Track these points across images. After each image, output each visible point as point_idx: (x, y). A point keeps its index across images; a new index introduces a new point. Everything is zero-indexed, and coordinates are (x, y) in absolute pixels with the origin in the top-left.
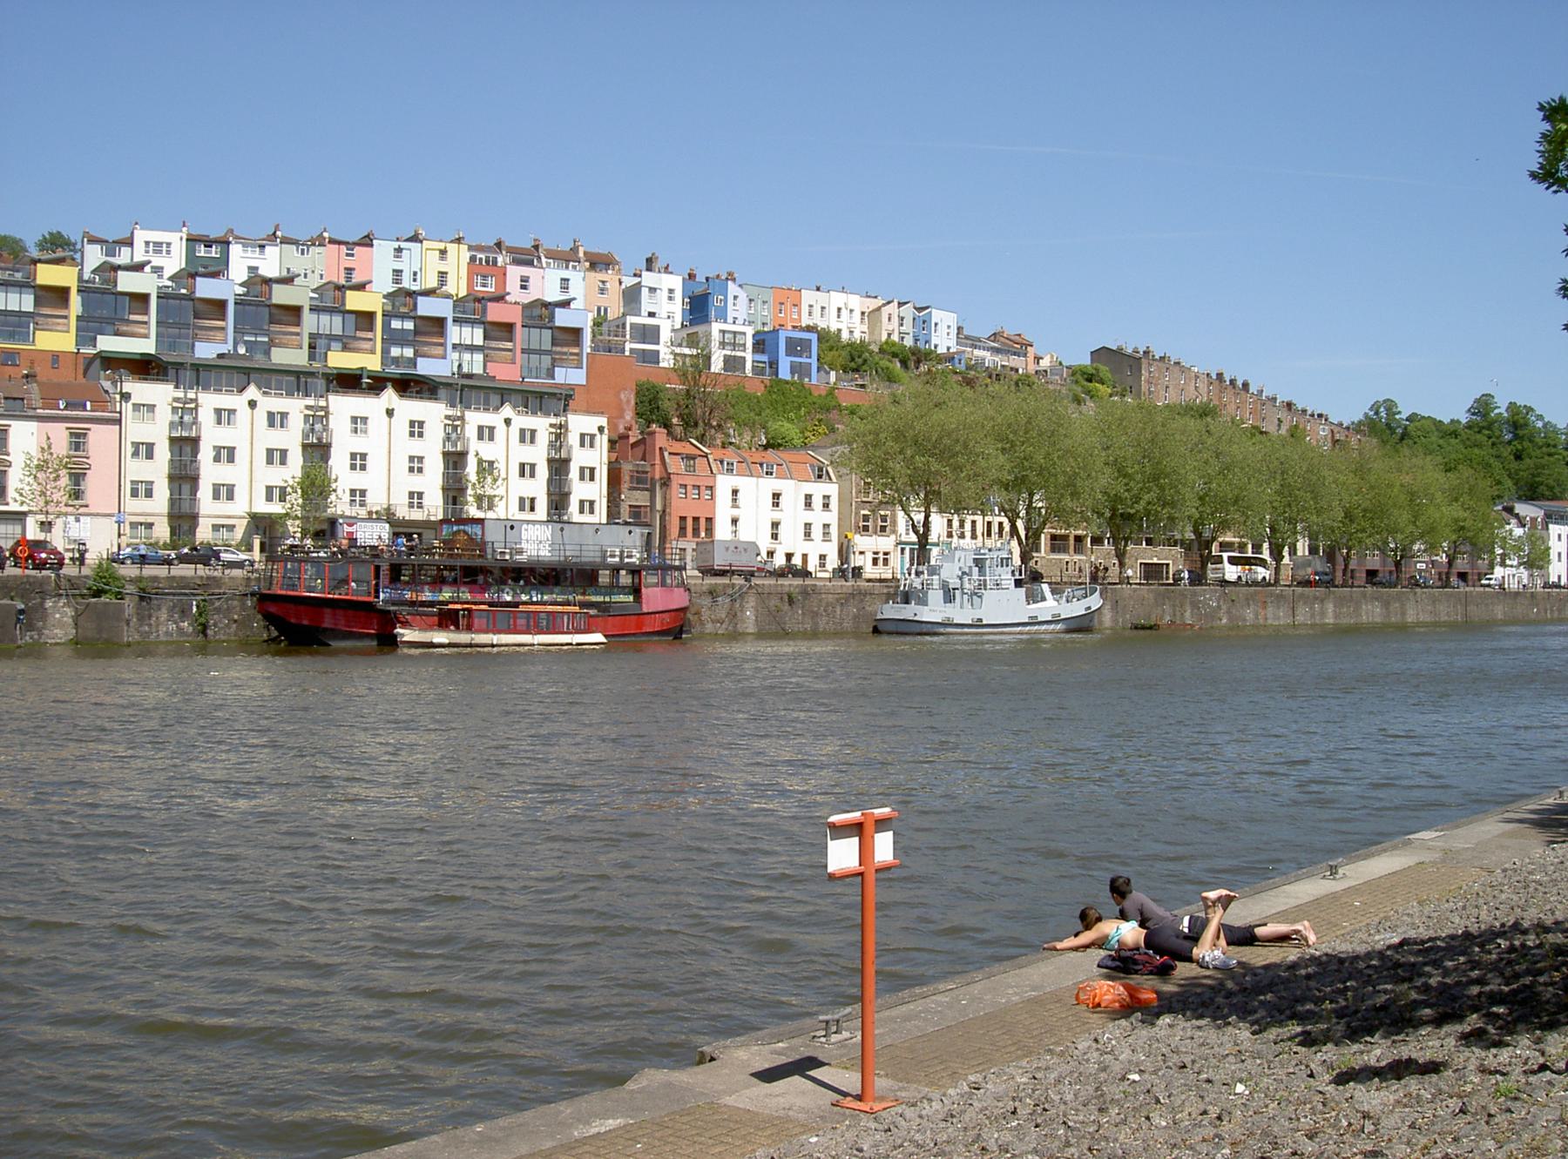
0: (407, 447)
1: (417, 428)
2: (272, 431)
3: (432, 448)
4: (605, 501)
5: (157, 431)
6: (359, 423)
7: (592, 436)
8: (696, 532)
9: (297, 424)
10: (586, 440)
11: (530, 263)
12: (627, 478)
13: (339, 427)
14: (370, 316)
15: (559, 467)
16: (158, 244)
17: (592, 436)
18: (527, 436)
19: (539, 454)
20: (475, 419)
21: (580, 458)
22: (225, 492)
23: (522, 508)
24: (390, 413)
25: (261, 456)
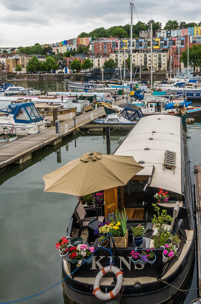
4: (167, 64)
6: (134, 56)
15: (160, 59)
16: (164, 32)
17: (165, 56)
20: (148, 55)
21: (163, 58)
23: (149, 65)
24: (137, 55)
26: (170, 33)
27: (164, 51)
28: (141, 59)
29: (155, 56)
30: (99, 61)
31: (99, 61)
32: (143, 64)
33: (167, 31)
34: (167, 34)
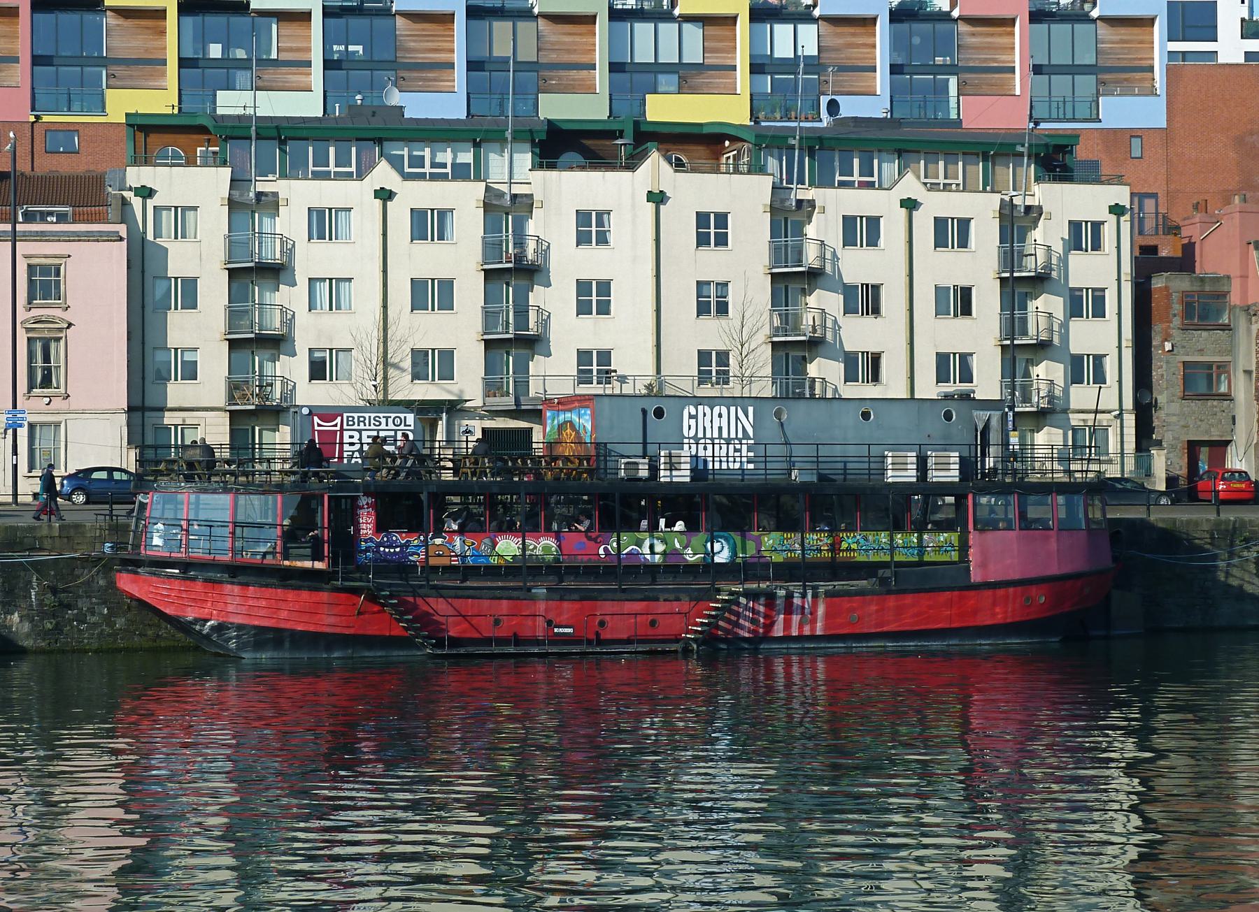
0: (690, 265)
1: (712, 229)
2: (422, 247)
5: (199, 256)
6: (591, 228)
7: (1097, 226)
9: (469, 224)
10: (1082, 236)
12: (1177, 308)
13: (551, 229)
14: (732, 20)
17: (1097, 226)
18: (952, 233)
19: (978, 265)
25: (401, 295)
28: (713, 264)
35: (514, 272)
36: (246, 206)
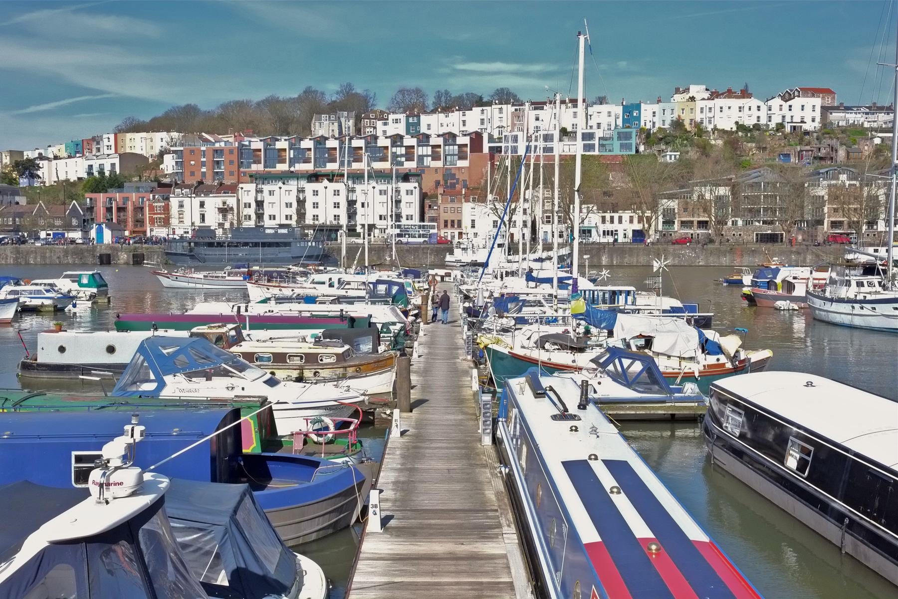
3: (342, 200)
5: (250, 198)
8: (453, 226)
11: (542, 109)
13: (309, 194)
21: (405, 198)
22: (272, 217)
24: (326, 188)
26: (419, 123)
27: (406, 178)
28: (337, 199)
29: (380, 191)
30: (202, 205)
31: (202, 205)
32: (344, 221)
33: (408, 117)
34: (408, 125)
35: (301, 203)
36: (259, 191)
